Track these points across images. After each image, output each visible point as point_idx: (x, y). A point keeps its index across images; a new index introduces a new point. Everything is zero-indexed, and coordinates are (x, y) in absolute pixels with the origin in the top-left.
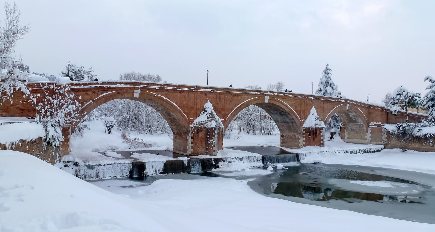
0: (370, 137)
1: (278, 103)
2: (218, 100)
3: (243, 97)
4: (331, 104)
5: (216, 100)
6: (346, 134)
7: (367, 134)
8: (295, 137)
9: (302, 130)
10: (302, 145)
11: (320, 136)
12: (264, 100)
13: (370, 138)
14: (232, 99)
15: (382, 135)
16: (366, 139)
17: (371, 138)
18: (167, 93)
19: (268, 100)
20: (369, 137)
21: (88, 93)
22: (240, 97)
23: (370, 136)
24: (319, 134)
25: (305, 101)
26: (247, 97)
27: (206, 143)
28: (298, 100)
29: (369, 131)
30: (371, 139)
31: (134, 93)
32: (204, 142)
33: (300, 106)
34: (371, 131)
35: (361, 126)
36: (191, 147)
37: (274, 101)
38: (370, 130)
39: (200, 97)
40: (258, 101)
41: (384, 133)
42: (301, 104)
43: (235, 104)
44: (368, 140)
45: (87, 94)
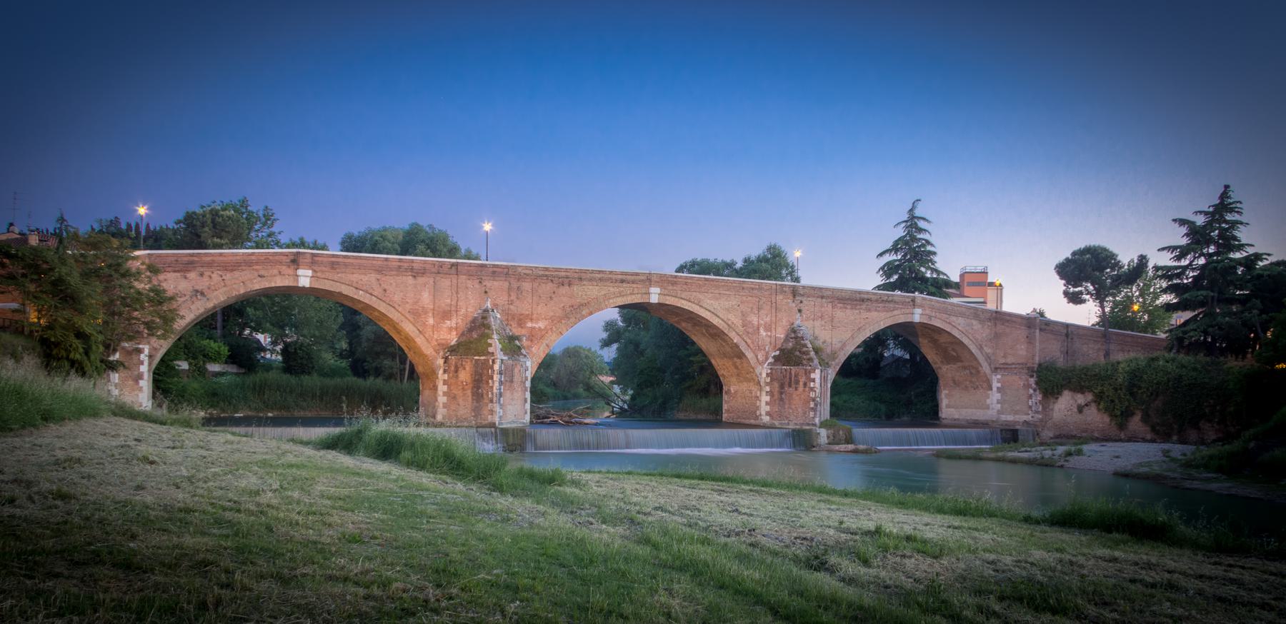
0: (998, 402)
1: (690, 304)
2: (513, 297)
4: (858, 307)
5: (510, 295)
6: (943, 396)
7: (990, 392)
8: (751, 392)
9: (764, 375)
10: (763, 413)
11: (807, 389)
12: (646, 296)
13: (998, 403)
15: (1030, 397)
16: (988, 407)
17: (999, 405)
18: (379, 277)
20: (995, 401)
21: (188, 275)
22: (575, 288)
23: (998, 400)
24: (805, 384)
25: (774, 301)
27: (473, 394)
28: (750, 298)
29: (996, 385)
30: (1002, 407)
31: (297, 276)
32: (469, 392)
34: (999, 385)
35: (973, 371)
36: (441, 405)
37: (677, 299)
38: (998, 382)
39: (467, 288)
41: (1035, 390)
42: (759, 309)
44: (993, 409)
45: (186, 278)
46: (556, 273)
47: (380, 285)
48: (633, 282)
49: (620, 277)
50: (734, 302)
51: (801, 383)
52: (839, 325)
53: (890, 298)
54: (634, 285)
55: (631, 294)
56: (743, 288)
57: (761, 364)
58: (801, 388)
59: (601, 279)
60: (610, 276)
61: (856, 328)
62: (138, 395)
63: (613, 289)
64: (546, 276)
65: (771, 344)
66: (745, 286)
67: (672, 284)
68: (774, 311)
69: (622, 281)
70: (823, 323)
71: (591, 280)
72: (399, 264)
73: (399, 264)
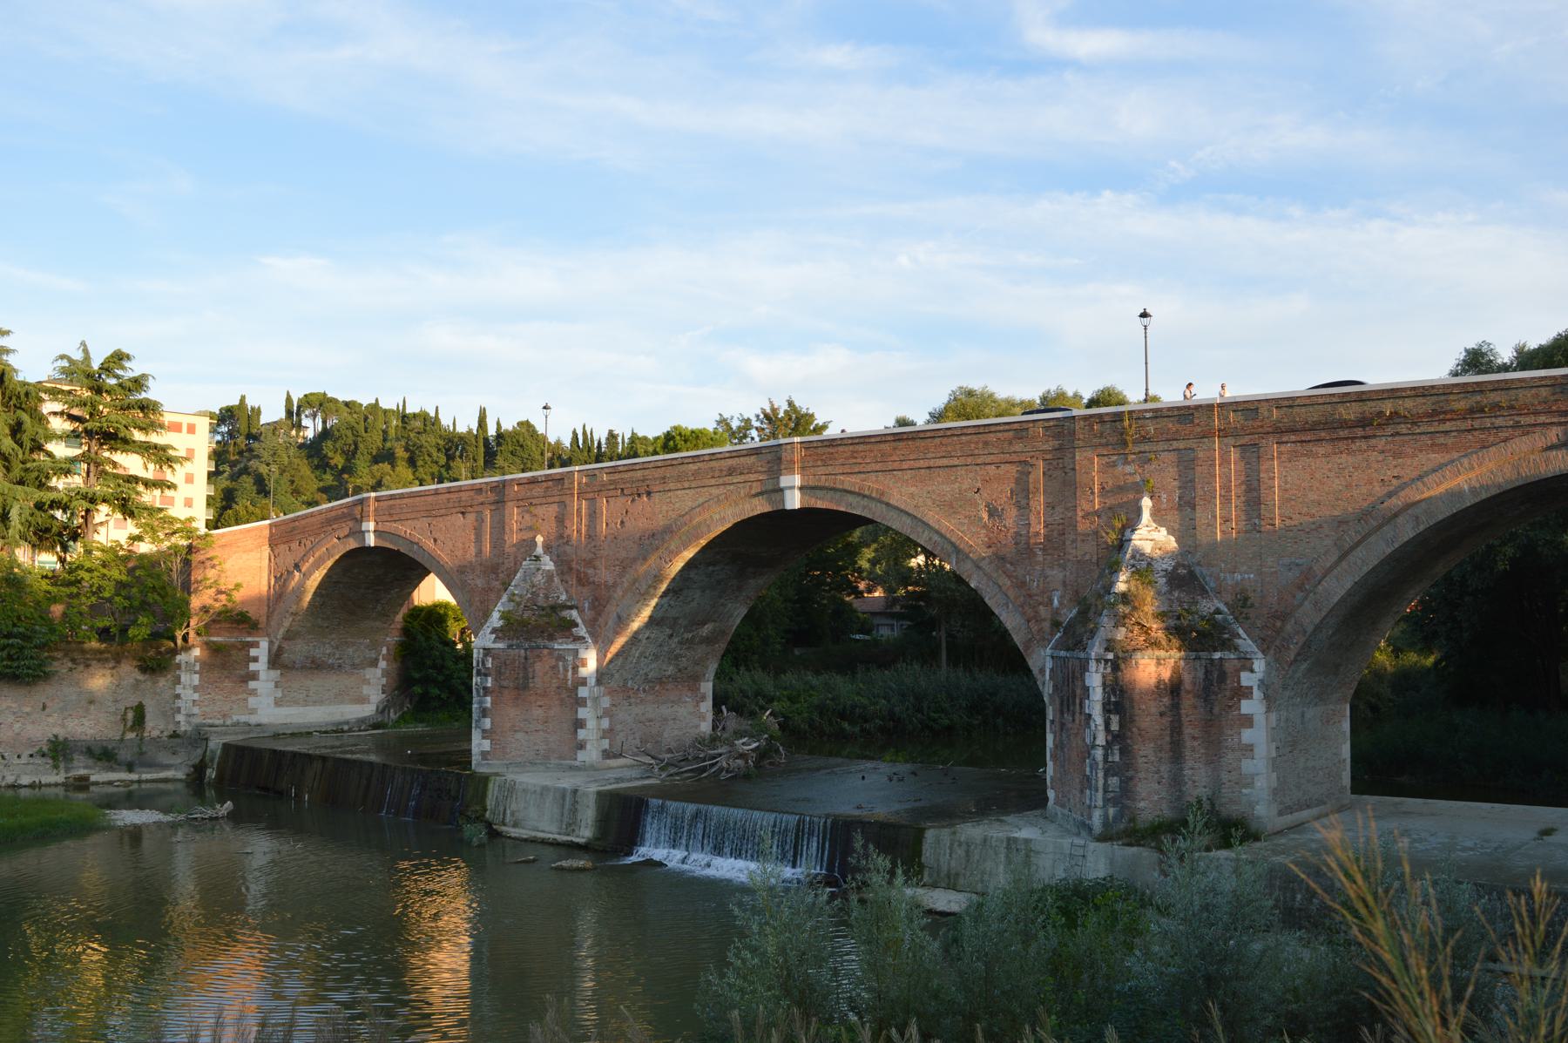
1: (865, 503)
12: (775, 496)
19: (797, 494)
46: (630, 474)
50: (967, 480)
51: (1078, 701)
57: (1044, 641)
58: (1077, 715)
60: (713, 464)
62: (246, 700)
65: (1064, 584)
69: (731, 471)
71: (679, 479)
73: (447, 496)
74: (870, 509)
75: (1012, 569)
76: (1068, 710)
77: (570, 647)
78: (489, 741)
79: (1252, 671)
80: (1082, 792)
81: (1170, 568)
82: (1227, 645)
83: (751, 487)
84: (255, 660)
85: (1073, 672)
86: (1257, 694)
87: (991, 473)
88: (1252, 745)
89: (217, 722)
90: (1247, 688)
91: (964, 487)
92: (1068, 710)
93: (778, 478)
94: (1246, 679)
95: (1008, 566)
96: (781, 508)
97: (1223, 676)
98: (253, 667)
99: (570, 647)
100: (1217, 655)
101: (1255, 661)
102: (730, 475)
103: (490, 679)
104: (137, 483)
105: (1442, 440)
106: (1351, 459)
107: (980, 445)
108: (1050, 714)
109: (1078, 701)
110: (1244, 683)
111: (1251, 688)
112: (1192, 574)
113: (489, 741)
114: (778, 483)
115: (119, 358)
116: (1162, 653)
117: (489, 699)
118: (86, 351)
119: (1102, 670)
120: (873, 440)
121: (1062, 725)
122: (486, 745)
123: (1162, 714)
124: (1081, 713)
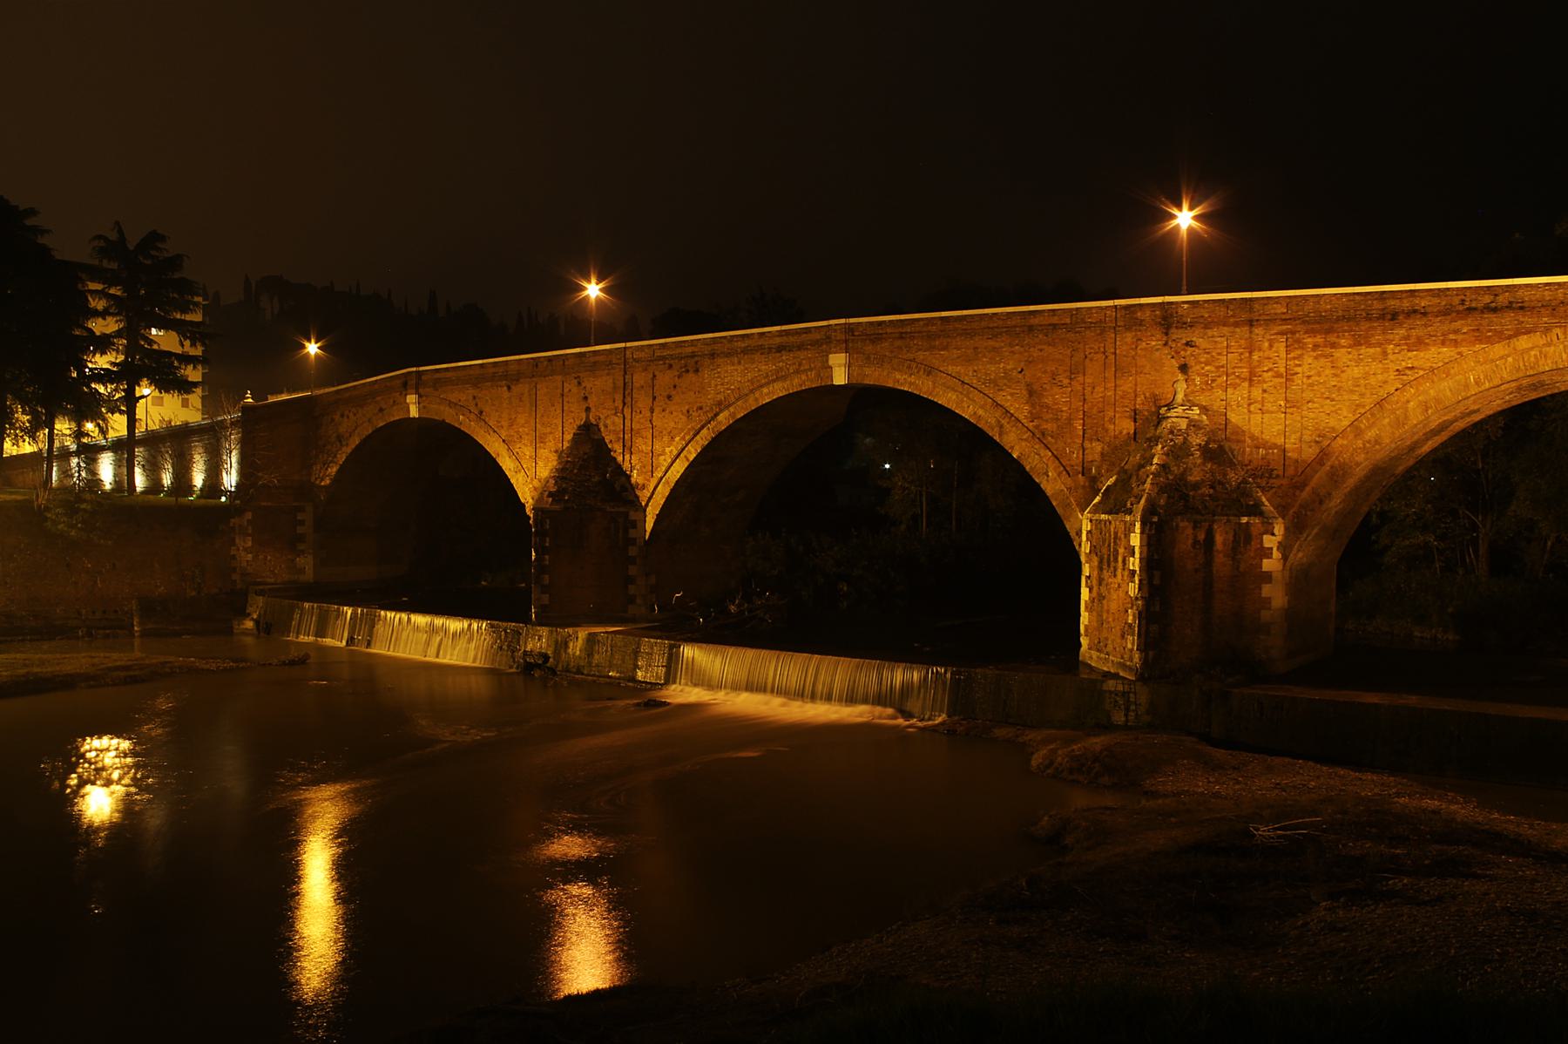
3: (718, 373)
14: (675, 387)
22: (706, 373)
26: (740, 368)
28: (1051, 349)
33: (1066, 381)
40: (796, 381)
43: (687, 407)
46: (679, 351)
47: (477, 405)
48: (800, 347)
49: (778, 340)
51: (1120, 559)
52: (1308, 395)
53: (1502, 299)
54: (802, 354)
55: (797, 372)
56: (1031, 328)
58: (1119, 572)
59: (745, 351)
61: (1369, 401)
63: (765, 366)
64: (663, 358)
66: (1034, 321)
67: (873, 342)
68: (1110, 373)
69: (780, 349)
70: (1257, 393)
71: (728, 355)
72: (494, 370)
73: (494, 370)
74: (917, 386)
75: (1053, 441)
76: (1109, 566)
77: (622, 509)
78: (548, 595)
79: (1273, 534)
80: (1123, 637)
81: (1203, 443)
82: (1256, 510)
83: (800, 365)
84: (302, 523)
85: (1116, 533)
86: (1276, 554)
87: (1035, 355)
88: (1270, 598)
89: (269, 580)
90: (1268, 548)
91: (1009, 367)
92: (1109, 566)
93: (827, 356)
94: (1269, 541)
95: (1050, 438)
96: (830, 383)
97: (1248, 538)
98: (300, 530)
99: (622, 509)
100: (1244, 520)
101: (1275, 525)
102: (780, 352)
103: (548, 539)
104: (170, 358)
105: (1452, 336)
106: (1372, 350)
107: (1026, 329)
108: (1086, 570)
109: (1120, 559)
110: (1266, 545)
111: (1272, 549)
112: (1221, 447)
113: (548, 595)
114: (827, 361)
115: (154, 238)
116: (1199, 517)
117: (547, 557)
118: (120, 232)
119: (1147, 531)
120: (921, 323)
121: (1100, 581)
122: (546, 599)
123: (1196, 571)
124: (1124, 569)
